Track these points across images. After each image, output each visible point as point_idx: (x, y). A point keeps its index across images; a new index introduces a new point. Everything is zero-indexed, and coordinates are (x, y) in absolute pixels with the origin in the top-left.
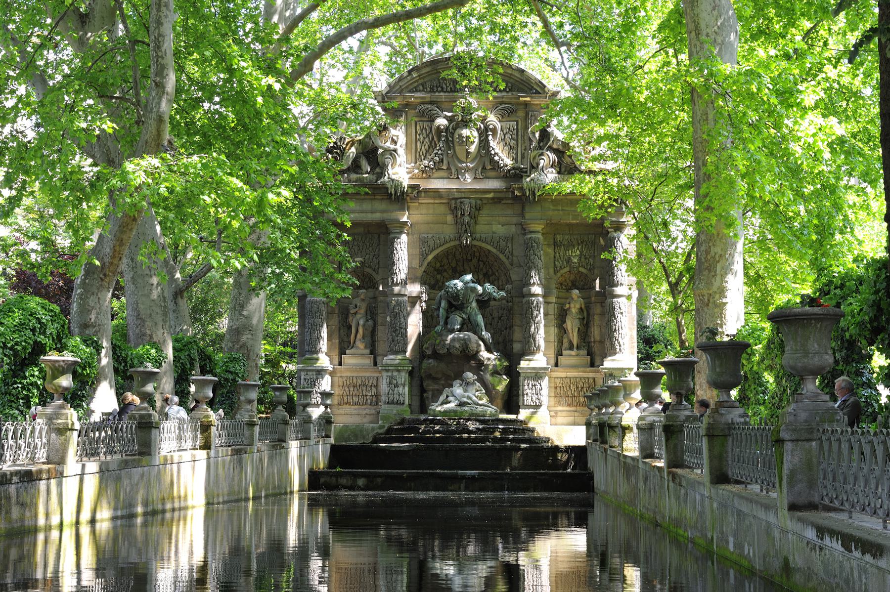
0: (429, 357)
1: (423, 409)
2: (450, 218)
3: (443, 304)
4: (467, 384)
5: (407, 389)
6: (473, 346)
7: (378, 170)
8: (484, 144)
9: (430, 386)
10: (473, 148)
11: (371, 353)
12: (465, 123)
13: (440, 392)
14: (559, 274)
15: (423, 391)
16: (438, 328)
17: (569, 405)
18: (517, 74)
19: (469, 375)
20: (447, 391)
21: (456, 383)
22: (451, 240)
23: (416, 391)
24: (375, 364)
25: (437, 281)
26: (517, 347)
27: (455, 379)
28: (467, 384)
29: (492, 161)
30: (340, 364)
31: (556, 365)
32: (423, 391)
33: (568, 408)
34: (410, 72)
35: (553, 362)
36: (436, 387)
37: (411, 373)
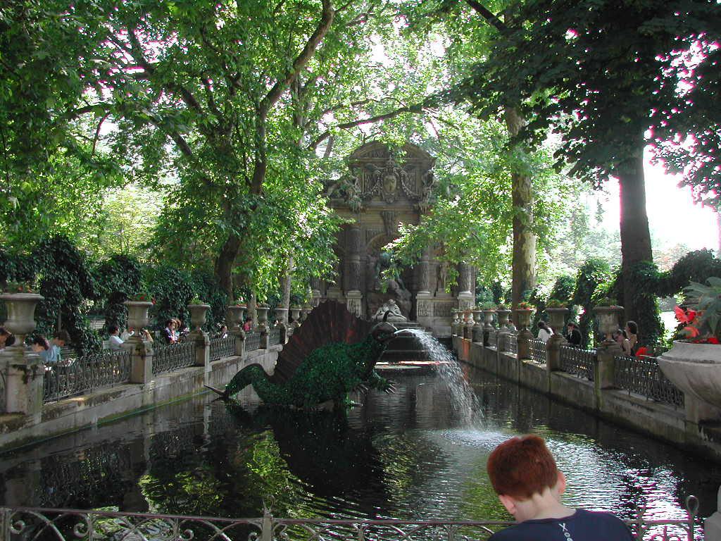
0: (370, 291)
1: (369, 317)
2: (381, 221)
3: (379, 265)
4: (390, 305)
5: (360, 308)
6: (394, 287)
7: (345, 197)
8: (399, 183)
9: (372, 306)
10: (394, 185)
11: (341, 289)
12: (391, 173)
13: (377, 310)
14: (436, 250)
15: (368, 308)
16: (377, 277)
17: (441, 316)
18: (415, 148)
19: (392, 301)
20: (381, 309)
21: (385, 304)
22: (382, 232)
23: (365, 310)
24: (343, 294)
25: (374, 253)
26: (415, 287)
27: (384, 302)
28: (391, 305)
29: (403, 191)
30: (326, 294)
31: (435, 295)
32: (368, 308)
33: (440, 318)
34: (362, 147)
35: (433, 294)
36: (374, 307)
37: (362, 300)
